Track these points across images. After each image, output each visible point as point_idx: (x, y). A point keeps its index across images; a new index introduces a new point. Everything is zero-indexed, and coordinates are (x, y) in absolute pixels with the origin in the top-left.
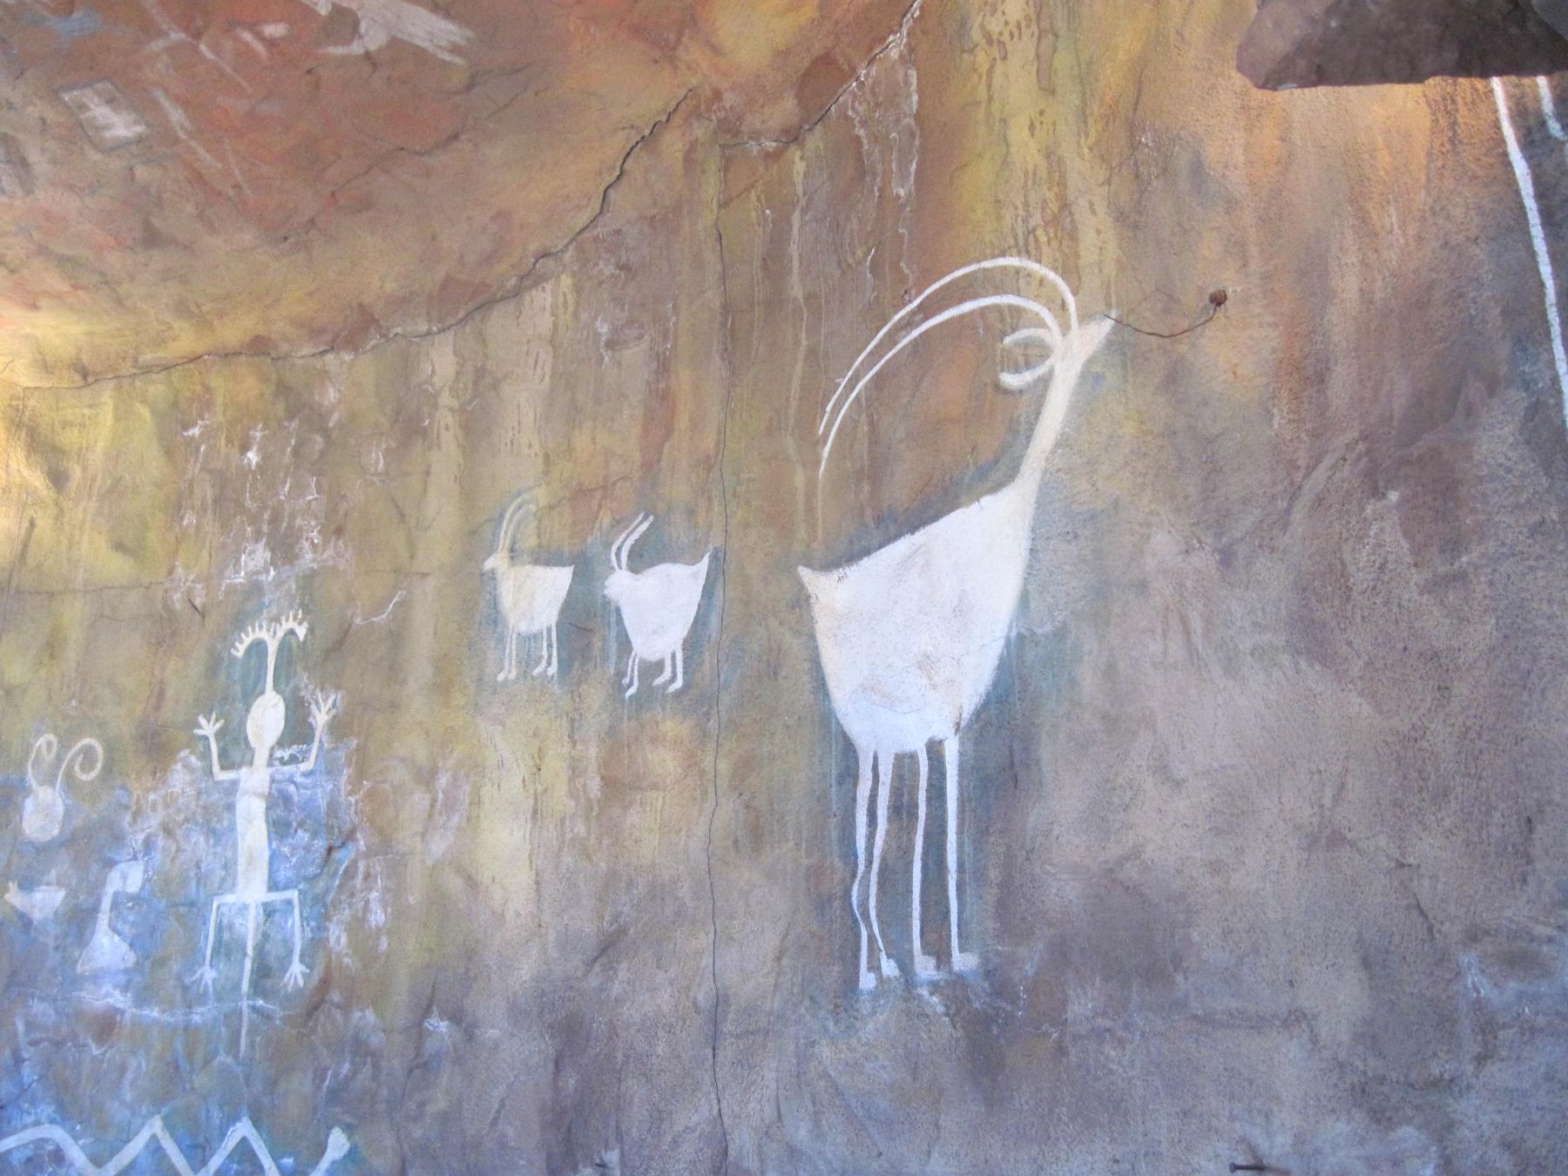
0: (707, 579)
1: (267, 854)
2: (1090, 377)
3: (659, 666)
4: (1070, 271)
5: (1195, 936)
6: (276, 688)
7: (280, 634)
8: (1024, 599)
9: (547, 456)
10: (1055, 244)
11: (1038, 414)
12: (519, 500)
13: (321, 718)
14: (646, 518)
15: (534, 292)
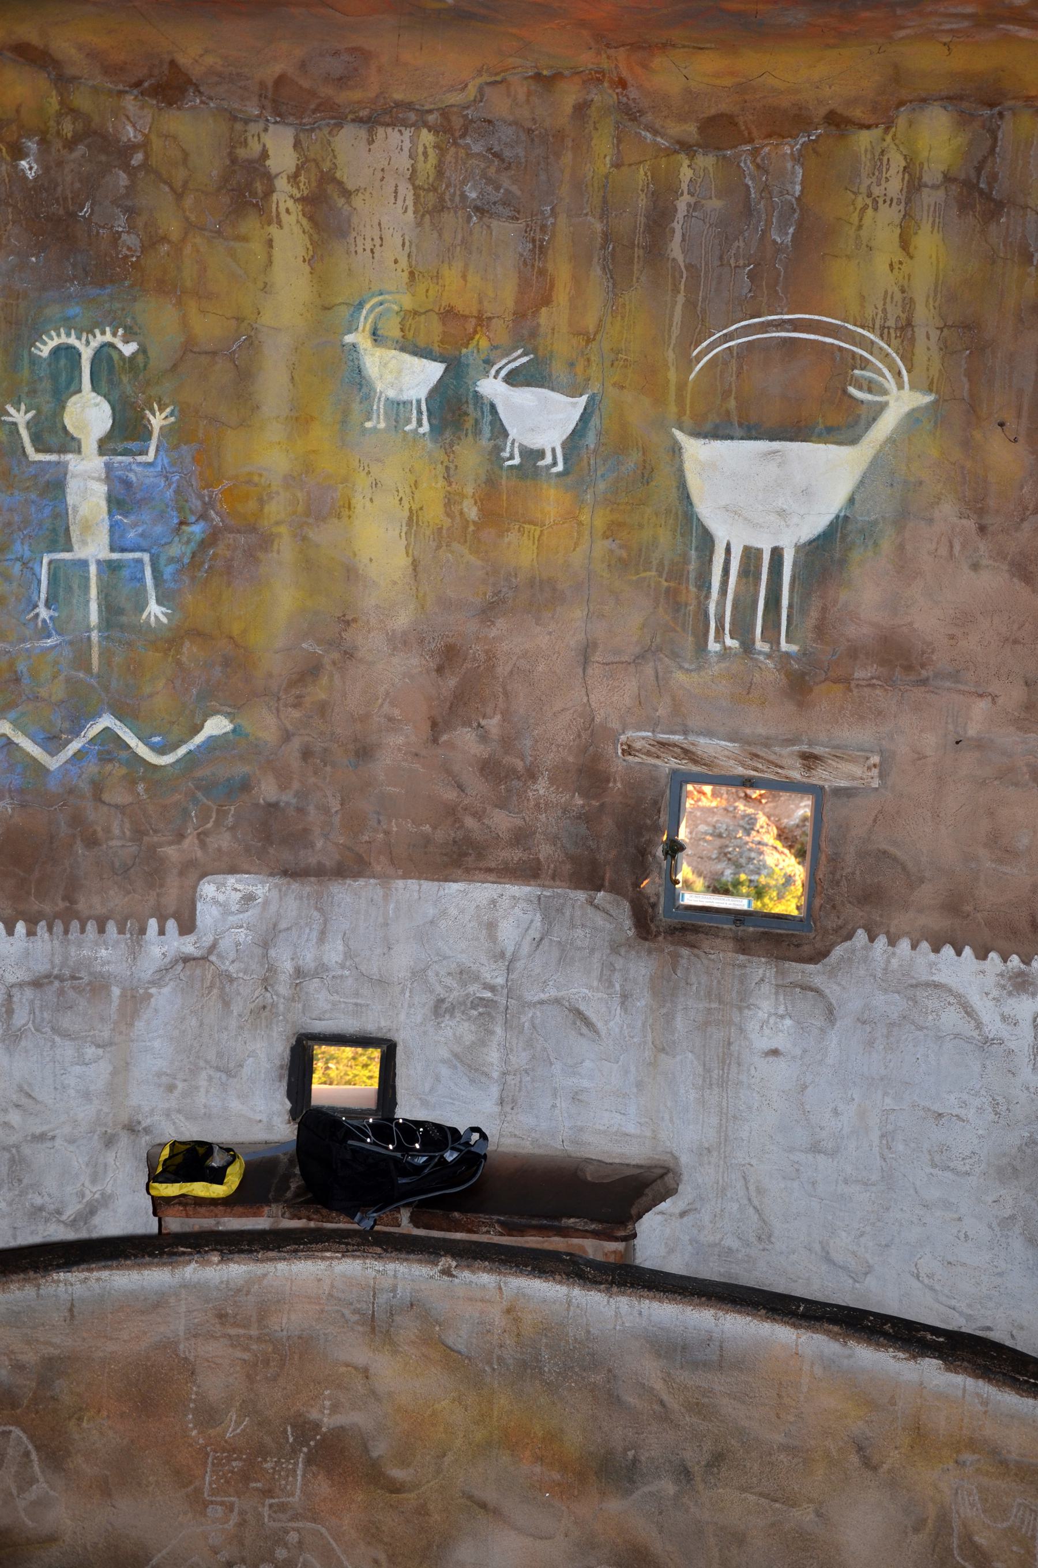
0: (585, 409)
1: (106, 524)
2: (913, 418)
3: (541, 454)
4: (908, 359)
5: (934, 658)
6: (95, 388)
7: (95, 344)
8: (851, 501)
9: (412, 274)
10: (899, 340)
11: (874, 420)
12: (380, 298)
13: (157, 421)
14: (524, 354)
15: (389, 130)
